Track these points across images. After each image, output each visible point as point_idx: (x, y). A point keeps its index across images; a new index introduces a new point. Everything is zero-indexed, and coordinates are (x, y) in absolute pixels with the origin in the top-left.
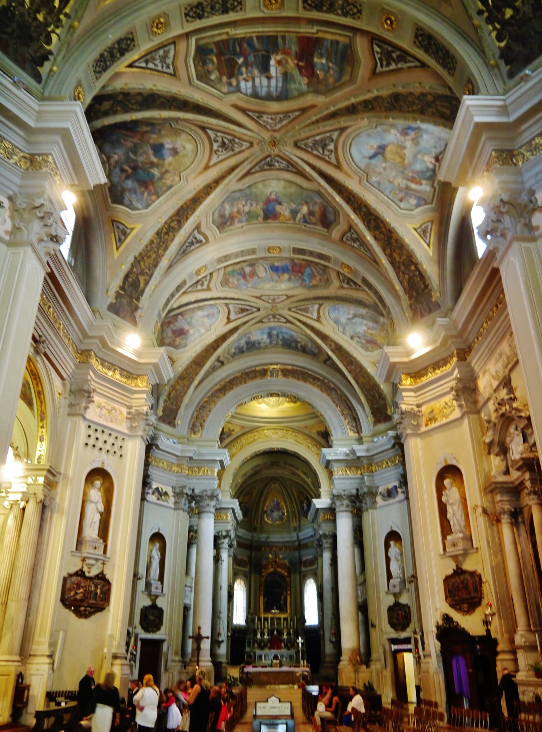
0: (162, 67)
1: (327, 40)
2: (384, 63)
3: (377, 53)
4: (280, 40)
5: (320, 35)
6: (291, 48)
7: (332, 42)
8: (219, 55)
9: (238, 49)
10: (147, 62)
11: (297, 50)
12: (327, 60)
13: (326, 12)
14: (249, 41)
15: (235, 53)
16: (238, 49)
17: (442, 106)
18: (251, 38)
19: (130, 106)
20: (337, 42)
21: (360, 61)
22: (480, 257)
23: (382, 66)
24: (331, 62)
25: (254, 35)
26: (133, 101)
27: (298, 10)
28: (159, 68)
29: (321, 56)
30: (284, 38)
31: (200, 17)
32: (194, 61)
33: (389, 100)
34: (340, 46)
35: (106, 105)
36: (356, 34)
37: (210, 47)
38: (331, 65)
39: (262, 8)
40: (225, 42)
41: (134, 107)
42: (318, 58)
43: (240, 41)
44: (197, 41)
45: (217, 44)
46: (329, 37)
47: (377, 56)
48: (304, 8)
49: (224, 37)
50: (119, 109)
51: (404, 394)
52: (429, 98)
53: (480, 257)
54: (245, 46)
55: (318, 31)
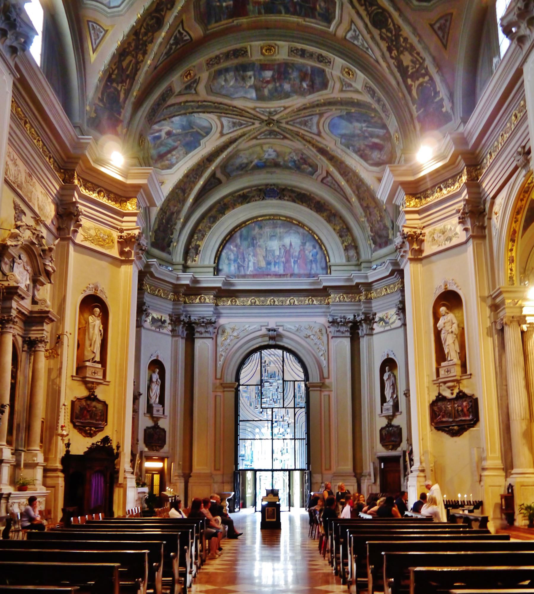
0: (358, 35)
1: (224, 20)
2: (178, 35)
3: (185, 36)
4: (263, 11)
5: (231, 20)
6: (254, 7)
7: (220, 20)
8: (314, 9)
9: (298, 8)
10: (367, 49)
11: (248, 7)
12: (221, 6)
13: (230, 51)
14: (288, 12)
15: (301, 7)
16: (298, 8)
17: (131, 61)
18: (286, 13)
19: (394, 33)
20: (216, 22)
21: (195, 20)
22: (39, 65)
23: (179, 31)
24: (218, 6)
25: (283, 14)
26: (389, 35)
27: (251, 46)
28: (360, 37)
29: (227, 7)
30: (260, 13)
31: (321, 55)
32: (335, 18)
33: (163, 13)
34: (213, 21)
35: (406, 59)
36: (204, 34)
37: (320, 18)
38: (218, 4)
39: (277, 47)
40: (306, 15)
41: (391, 26)
42: (230, 5)
43: (295, 13)
44: (329, 28)
45: (314, 17)
46: (223, 22)
47: (185, 33)
48: (246, 48)
49: (307, 19)
50: (402, 40)
51: (241, 423)
52: (140, 57)
53: (39, 65)
54: (291, 9)
55: (233, 22)
